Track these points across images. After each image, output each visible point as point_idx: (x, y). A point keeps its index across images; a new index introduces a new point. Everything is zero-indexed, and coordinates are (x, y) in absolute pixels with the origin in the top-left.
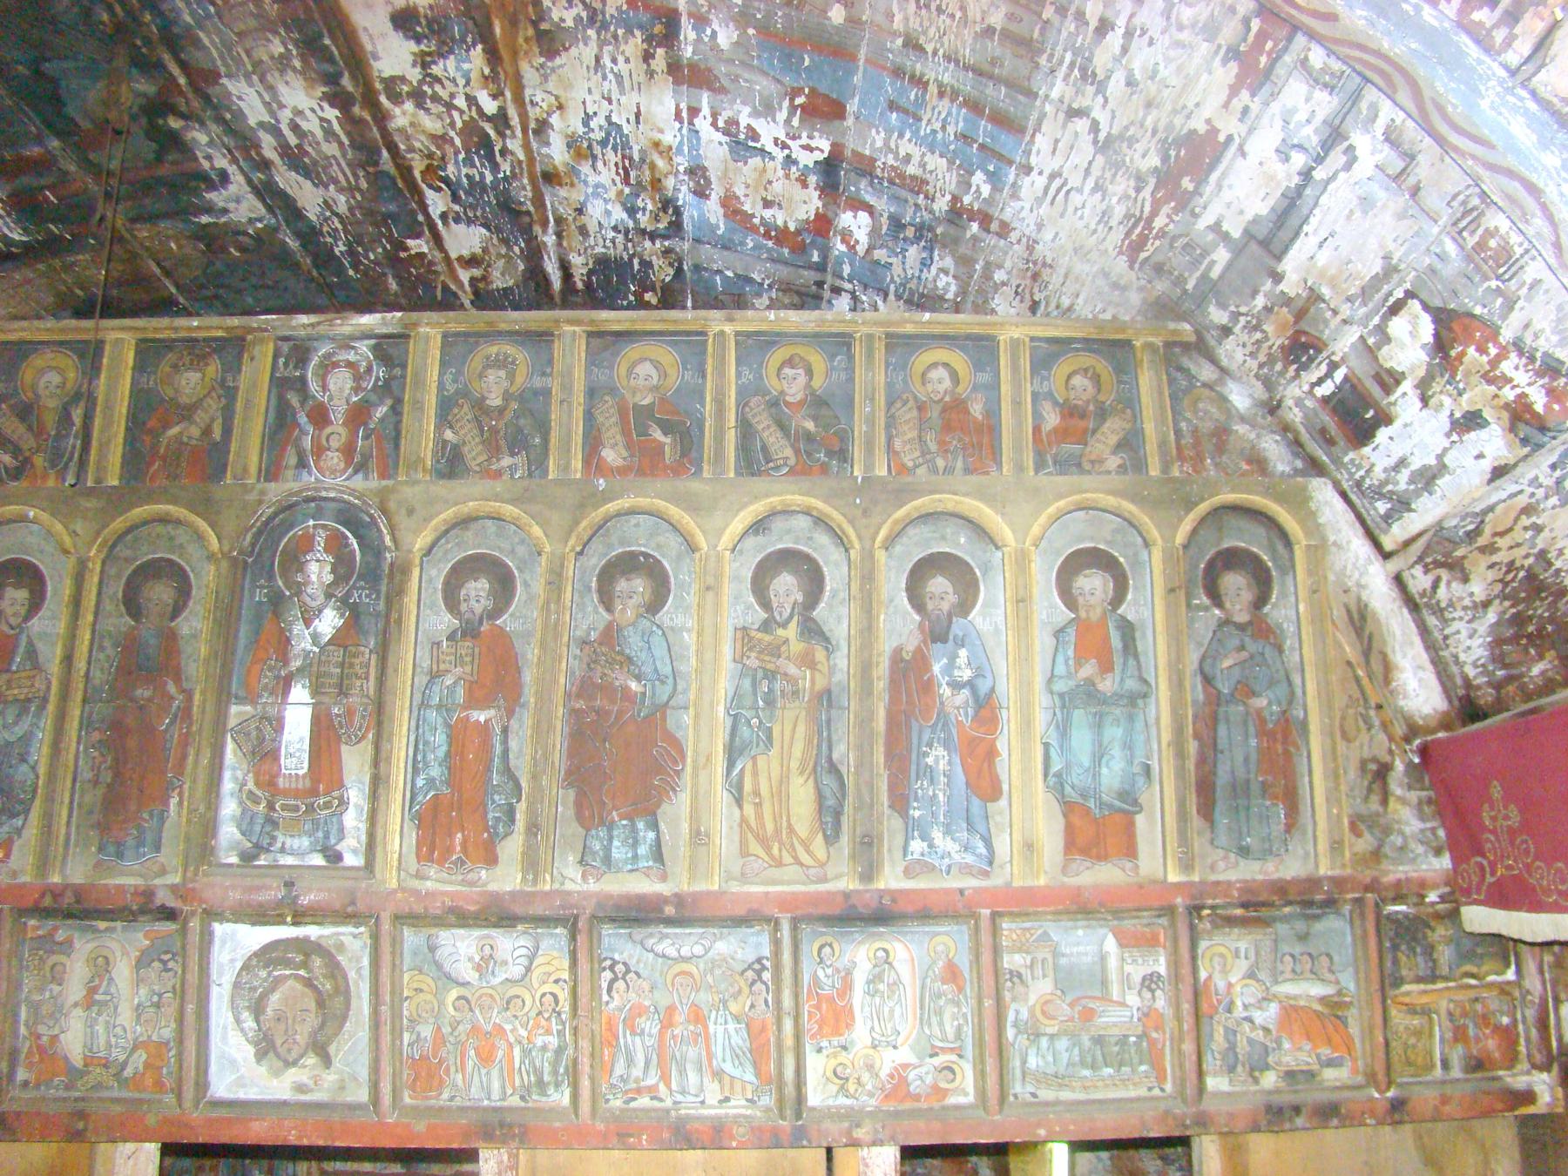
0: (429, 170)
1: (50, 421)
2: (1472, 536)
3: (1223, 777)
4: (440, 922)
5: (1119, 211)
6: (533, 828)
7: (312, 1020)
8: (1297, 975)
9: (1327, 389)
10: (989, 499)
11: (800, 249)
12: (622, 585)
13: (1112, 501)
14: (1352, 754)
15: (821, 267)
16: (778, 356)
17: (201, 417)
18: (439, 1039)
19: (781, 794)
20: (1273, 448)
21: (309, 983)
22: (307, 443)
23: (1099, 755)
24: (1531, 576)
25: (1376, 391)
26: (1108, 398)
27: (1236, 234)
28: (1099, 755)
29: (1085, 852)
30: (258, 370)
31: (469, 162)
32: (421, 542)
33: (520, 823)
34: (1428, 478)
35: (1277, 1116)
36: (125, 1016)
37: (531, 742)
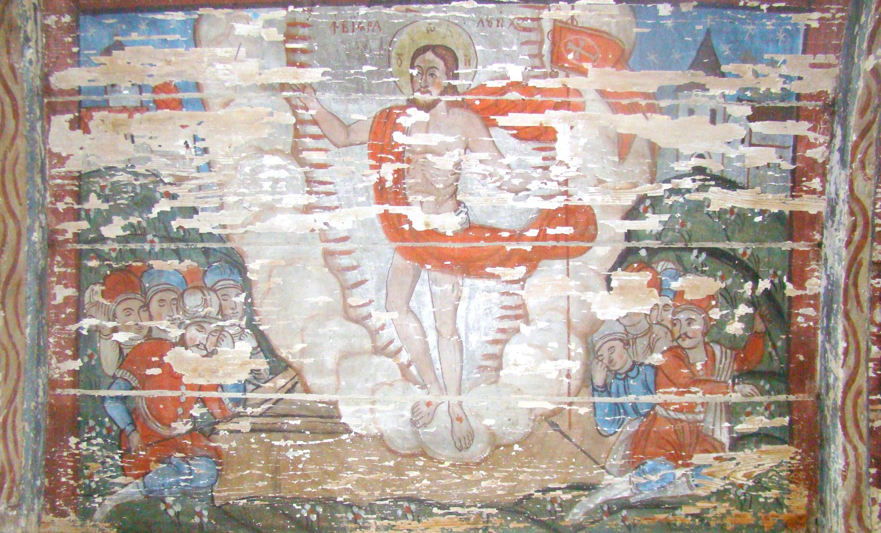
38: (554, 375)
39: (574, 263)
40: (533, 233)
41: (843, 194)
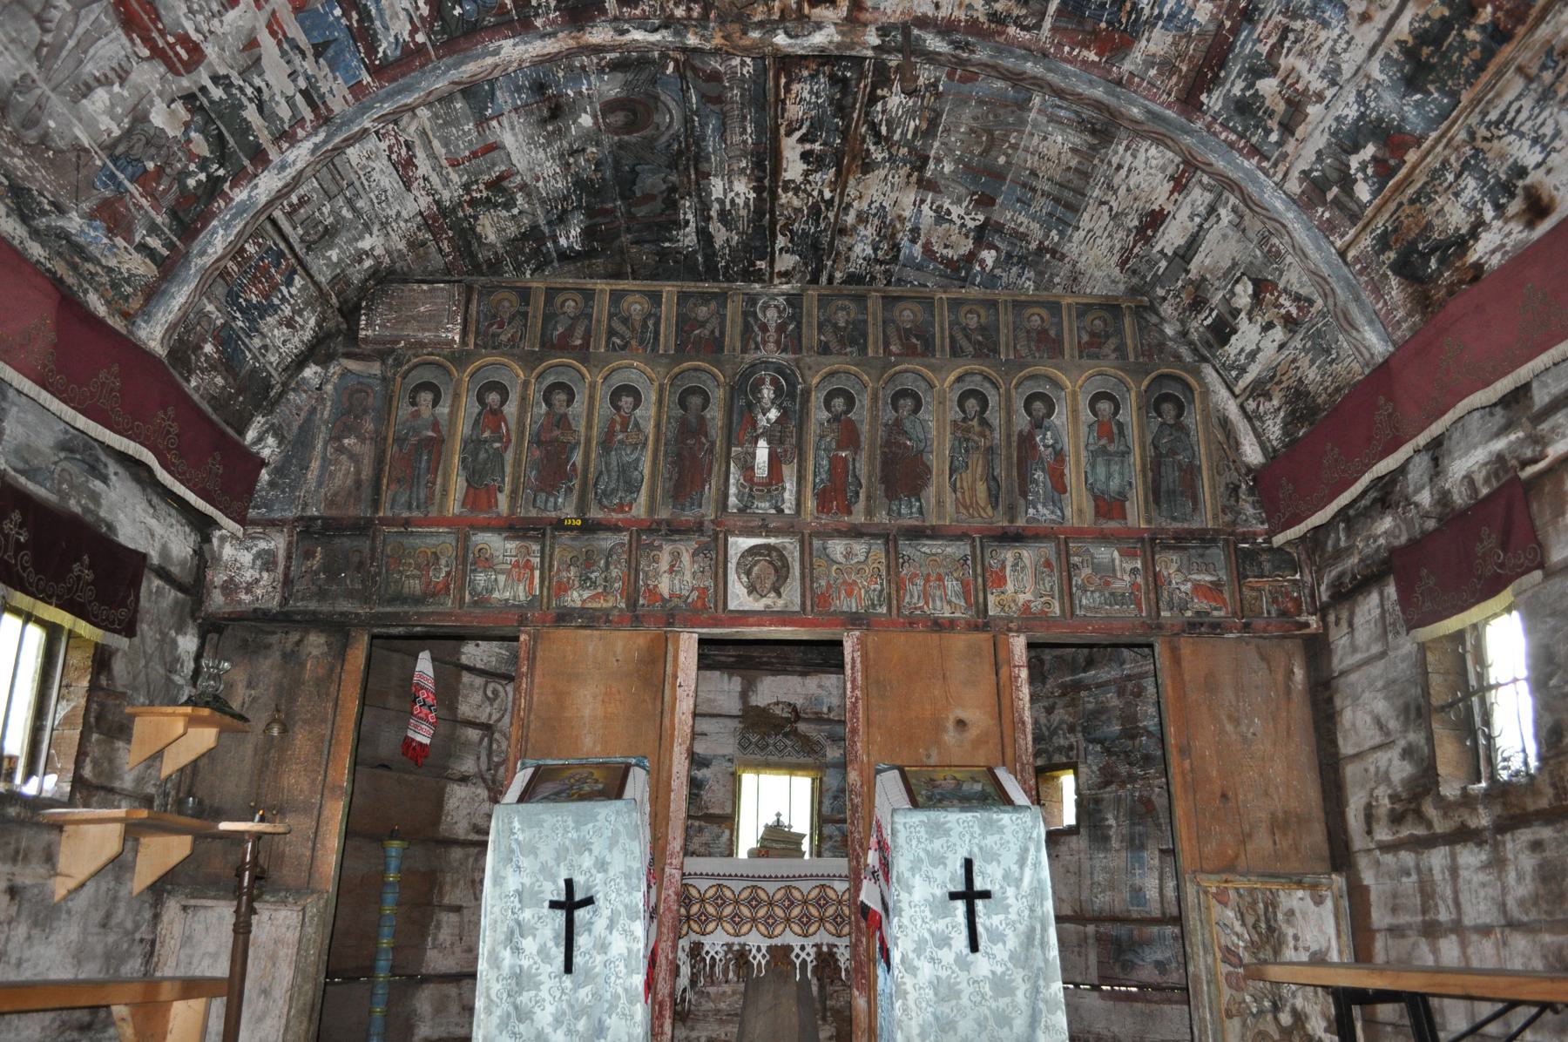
0: (785, 226)
1: (638, 325)
2: (1272, 378)
3: (1164, 487)
4: (831, 536)
5: (1118, 246)
6: (868, 498)
7: (773, 578)
8: (1199, 572)
9: (1209, 321)
10: (1060, 370)
11: (957, 270)
14: (1222, 481)
15: (964, 280)
16: (965, 308)
17: (709, 326)
19: (973, 489)
20: (1184, 351)
21: (770, 563)
23: (1109, 476)
24: (1297, 390)
25: (1230, 318)
26: (1111, 330)
28: (1109, 476)
29: (1104, 516)
30: (733, 309)
31: (806, 223)
32: (815, 381)
34: (1252, 356)
35: (1192, 626)
36: (688, 577)
37: (863, 466)
38: (103, 128)
39: (170, 76)
40: (171, 39)
41: (299, 166)
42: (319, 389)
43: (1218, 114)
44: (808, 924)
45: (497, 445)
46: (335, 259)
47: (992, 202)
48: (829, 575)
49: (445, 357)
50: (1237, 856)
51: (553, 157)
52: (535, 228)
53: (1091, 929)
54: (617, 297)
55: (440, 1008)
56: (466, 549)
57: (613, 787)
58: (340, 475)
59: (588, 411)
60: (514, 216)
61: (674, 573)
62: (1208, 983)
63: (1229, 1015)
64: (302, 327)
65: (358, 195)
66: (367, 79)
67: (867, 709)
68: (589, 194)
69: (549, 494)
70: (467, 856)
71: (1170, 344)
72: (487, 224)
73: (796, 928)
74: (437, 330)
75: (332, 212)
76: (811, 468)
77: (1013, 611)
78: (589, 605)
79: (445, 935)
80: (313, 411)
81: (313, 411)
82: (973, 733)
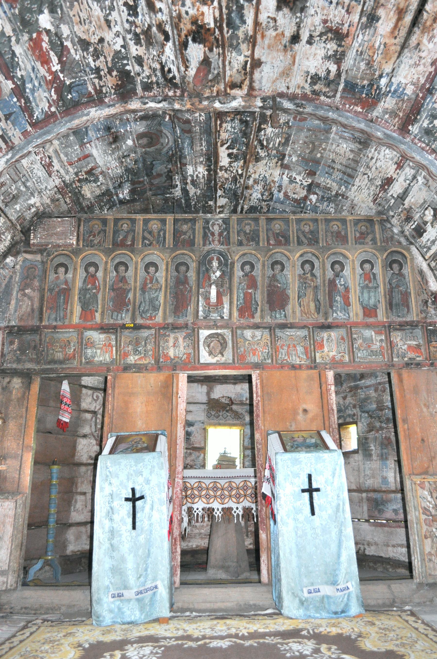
0: (221, 186)
1: (156, 234)
3: (394, 302)
4: (245, 328)
5: (372, 193)
6: (262, 311)
7: (220, 348)
8: (410, 340)
9: (413, 227)
10: (347, 250)
11: (300, 204)
12: (276, 266)
13: (370, 250)
14: (420, 299)
15: (303, 208)
16: (303, 223)
17: (188, 234)
18: (245, 351)
19: (308, 305)
20: (402, 240)
21: (218, 341)
22: (211, 239)
23: (369, 298)
25: (423, 226)
26: (369, 231)
27: (396, 196)
28: (369, 298)
30: (199, 226)
31: (231, 184)
32: (236, 258)
33: (259, 310)
35: (407, 365)
36: (182, 348)
37: (259, 296)
42: (13, 267)
43: (417, 135)
44: (239, 498)
45: (94, 291)
46: (18, 209)
47: (315, 174)
48: (244, 346)
49: (70, 251)
50: (428, 467)
51: (115, 159)
52: (108, 190)
53: (364, 495)
54: (146, 222)
55: (78, 537)
56: (82, 339)
57: (151, 447)
58: (24, 306)
59: (135, 274)
60: (98, 186)
61: (176, 347)
62: (417, 524)
63: (426, 537)
64: (5, 240)
65: (27, 180)
66: (29, 129)
67: (263, 405)
68: (132, 174)
69: (118, 312)
70: (88, 470)
71: (396, 236)
72: (86, 189)
73: (234, 500)
74: (65, 239)
75: (16, 188)
76: (235, 298)
77: (328, 360)
78: (138, 362)
79: (79, 505)
80: (11, 277)
81: (11, 277)
82: (310, 415)
